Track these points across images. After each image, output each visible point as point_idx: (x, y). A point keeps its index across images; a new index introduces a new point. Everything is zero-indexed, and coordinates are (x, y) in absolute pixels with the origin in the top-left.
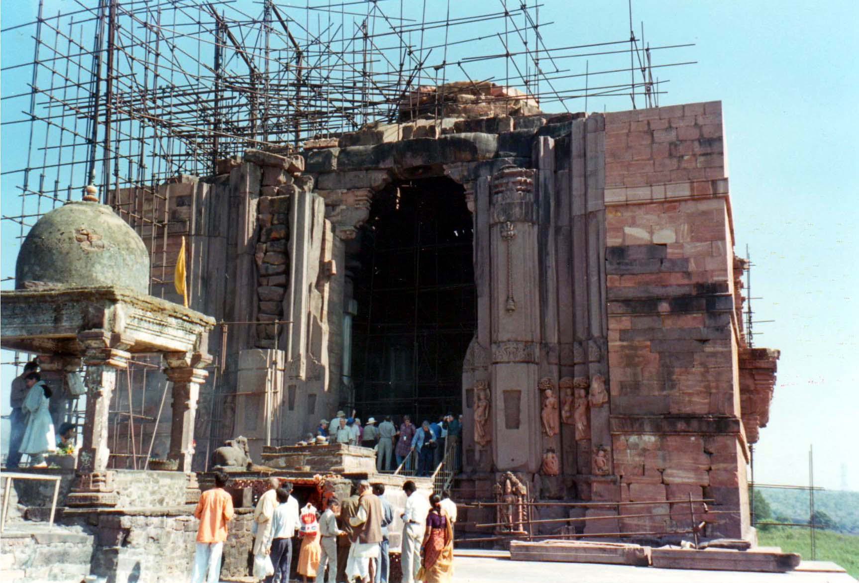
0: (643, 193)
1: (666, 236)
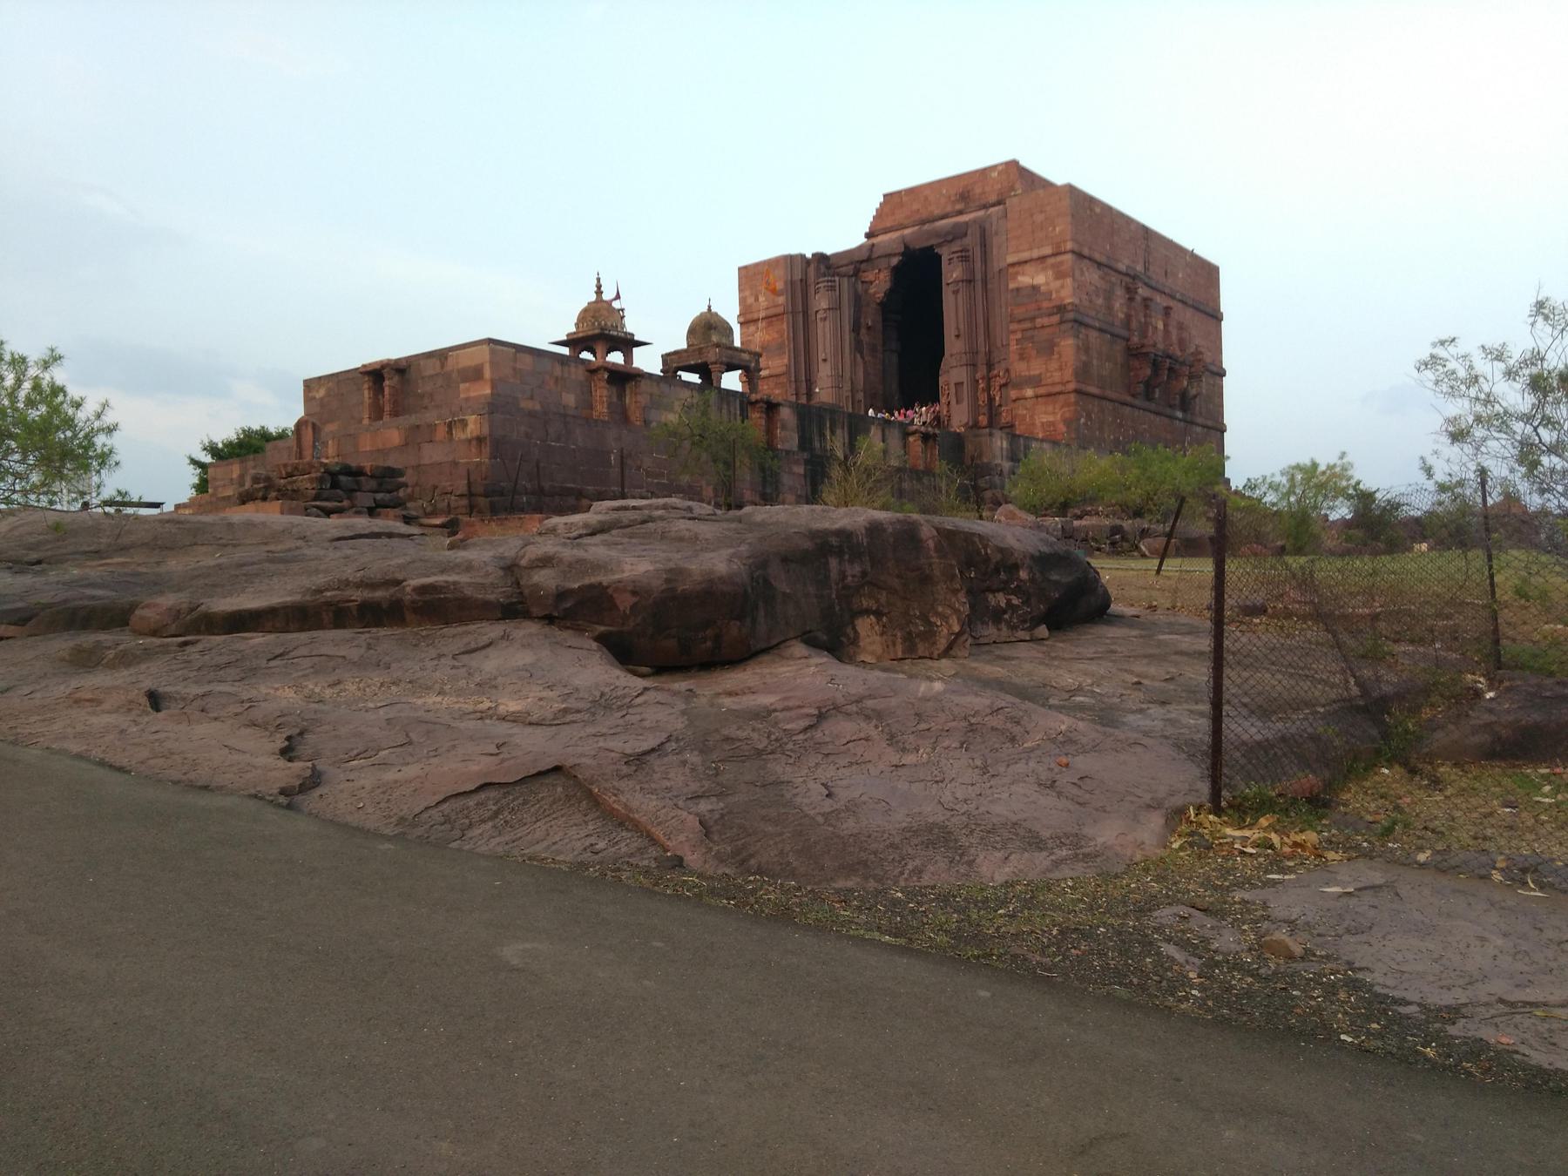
0: (1026, 255)
1: (1040, 279)
